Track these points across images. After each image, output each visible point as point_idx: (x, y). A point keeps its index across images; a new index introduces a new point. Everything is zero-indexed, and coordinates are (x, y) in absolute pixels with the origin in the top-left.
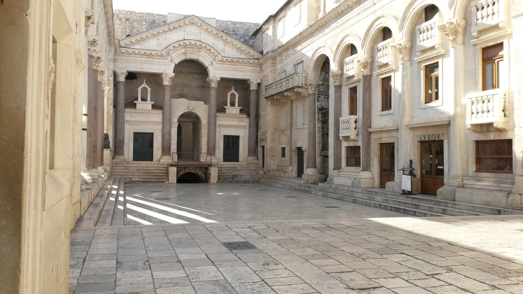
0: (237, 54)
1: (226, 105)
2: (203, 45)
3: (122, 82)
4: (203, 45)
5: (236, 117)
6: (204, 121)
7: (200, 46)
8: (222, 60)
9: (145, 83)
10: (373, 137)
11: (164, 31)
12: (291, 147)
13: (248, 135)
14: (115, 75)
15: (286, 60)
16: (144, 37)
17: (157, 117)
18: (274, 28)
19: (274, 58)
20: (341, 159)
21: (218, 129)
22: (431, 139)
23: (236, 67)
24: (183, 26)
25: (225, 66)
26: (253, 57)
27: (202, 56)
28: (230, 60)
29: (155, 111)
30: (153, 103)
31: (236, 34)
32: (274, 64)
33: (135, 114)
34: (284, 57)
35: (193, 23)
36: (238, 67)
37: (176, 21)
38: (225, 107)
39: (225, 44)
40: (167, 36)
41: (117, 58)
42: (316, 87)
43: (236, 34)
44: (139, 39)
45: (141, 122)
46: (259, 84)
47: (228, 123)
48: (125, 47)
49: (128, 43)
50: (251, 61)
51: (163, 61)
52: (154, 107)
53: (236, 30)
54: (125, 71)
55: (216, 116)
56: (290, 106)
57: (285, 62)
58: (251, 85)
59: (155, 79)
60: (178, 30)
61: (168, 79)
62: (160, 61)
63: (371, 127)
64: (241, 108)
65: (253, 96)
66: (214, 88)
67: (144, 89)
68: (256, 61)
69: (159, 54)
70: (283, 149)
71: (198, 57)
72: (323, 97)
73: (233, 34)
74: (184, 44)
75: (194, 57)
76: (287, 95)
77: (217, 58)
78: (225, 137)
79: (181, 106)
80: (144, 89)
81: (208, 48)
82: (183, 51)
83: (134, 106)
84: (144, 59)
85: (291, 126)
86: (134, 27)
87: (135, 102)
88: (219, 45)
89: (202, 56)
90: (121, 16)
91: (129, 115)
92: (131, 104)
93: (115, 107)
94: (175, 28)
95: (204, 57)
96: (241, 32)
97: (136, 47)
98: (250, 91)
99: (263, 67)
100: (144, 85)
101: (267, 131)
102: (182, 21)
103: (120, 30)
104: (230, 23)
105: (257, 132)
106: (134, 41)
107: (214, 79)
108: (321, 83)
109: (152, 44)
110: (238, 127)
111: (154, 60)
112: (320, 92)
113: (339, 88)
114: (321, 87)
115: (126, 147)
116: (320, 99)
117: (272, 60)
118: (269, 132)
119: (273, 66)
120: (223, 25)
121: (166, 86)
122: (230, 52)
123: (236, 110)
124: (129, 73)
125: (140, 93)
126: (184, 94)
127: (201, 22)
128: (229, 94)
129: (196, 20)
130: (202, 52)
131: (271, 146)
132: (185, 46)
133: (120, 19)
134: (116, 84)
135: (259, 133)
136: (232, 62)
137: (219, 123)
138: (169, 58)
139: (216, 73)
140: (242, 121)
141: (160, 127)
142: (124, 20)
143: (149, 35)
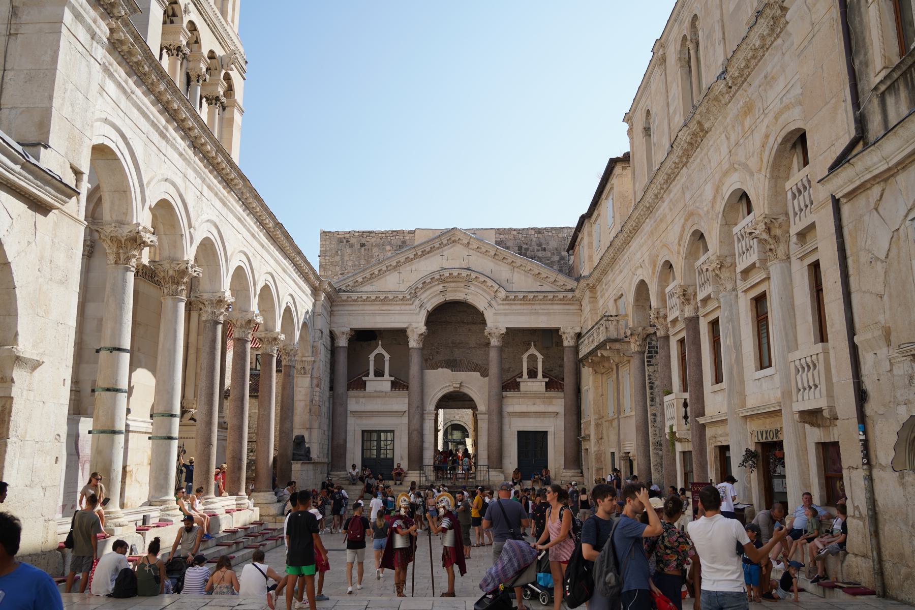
1: (521, 377)
3: (344, 347)
4: (473, 275)
5: (539, 398)
6: (482, 407)
7: (468, 276)
9: (380, 346)
10: (709, 432)
11: (408, 260)
12: (620, 451)
14: (332, 336)
15: (607, 290)
16: (376, 273)
17: (400, 403)
18: (590, 235)
19: (593, 289)
20: (676, 478)
21: (506, 420)
22: (770, 440)
23: (534, 307)
24: (438, 248)
25: (514, 307)
26: (565, 288)
30: (393, 379)
31: (544, 250)
32: (594, 299)
36: (537, 307)
37: (425, 243)
38: (518, 380)
40: (414, 267)
41: (335, 309)
42: (644, 339)
43: (544, 250)
45: (373, 413)
46: (579, 336)
48: (348, 291)
49: (351, 284)
50: (561, 296)
51: (407, 307)
52: (395, 385)
53: (543, 241)
55: (501, 399)
56: (615, 376)
58: (564, 337)
59: (396, 337)
61: (416, 337)
62: (403, 307)
63: (703, 414)
64: (547, 380)
67: (379, 358)
68: (570, 295)
70: (613, 453)
73: (538, 250)
74: (443, 278)
75: (459, 296)
76: (602, 355)
77: (499, 294)
78: (520, 434)
80: (379, 358)
81: (482, 278)
82: (440, 287)
83: (363, 386)
85: (619, 412)
86: (372, 256)
87: (364, 379)
88: (503, 272)
90: (353, 241)
91: (355, 403)
92: (356, 383)
93: (331, 389)
94: (424, 253)
96: (553, 244)
97: (365, 289)
98: (563, 348)
100: (380, 350)
103: (350, 263)
104: (533, 232)
105: (579, 424)
106: (360, 280)
107: (496, 331)
109: (392, 282)
110: (543, 414)
111: (393, 308)
112: (653, 347)
113: (667, 338)
116: (653, 361)
119: (593, 302)
120: (520, 236)
122: (522, 281)
125: (372, 363)
126: (455, 360)
128: (525, 357)
130: (473, 288)
131: (595, 449)
132: (442, 280)
133: (352, 246)
134: (333, 350)
136: (527, 299)
138: (417, 302)
139: (498, 320)
141: (405, 420)
142: (357, 246)
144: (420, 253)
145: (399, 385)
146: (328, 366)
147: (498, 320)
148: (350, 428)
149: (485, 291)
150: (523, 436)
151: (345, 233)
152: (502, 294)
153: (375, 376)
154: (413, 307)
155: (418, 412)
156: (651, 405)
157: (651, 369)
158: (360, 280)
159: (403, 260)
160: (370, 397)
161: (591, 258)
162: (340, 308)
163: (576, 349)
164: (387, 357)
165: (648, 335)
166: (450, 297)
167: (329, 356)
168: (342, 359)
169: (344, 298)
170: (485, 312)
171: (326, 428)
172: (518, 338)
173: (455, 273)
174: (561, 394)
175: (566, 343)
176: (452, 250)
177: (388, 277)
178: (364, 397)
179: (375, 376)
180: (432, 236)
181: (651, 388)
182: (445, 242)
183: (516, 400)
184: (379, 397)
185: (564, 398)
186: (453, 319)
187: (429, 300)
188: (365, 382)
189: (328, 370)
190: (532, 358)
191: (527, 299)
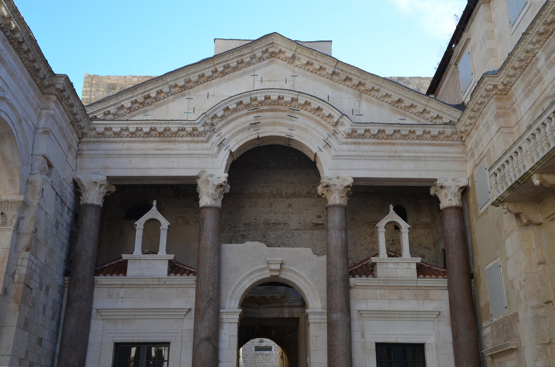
0: (396, 118)
1: (377, 255)
3: (92, 205)
4: (302, 101)
5: (408, 288)
6: (316, 303)
7: (293, 105)
8: (352, 134)
9: (154, 208)
13: (449, 337)
16: (153, 95)
17: (183, 295)
18: (489, 20)
19: (505, 92)
21: (356, 325)
23: (393, 148)
24: (249, 64)
25: (365, 147)
27: (301, 128)
29: (178, 279)
30: (171, 257)
33: (122, 292)
34: (541, 63)
36: (399, 148)
38: (374, 260)
39: (360, 96)
40: (211, 91)
41: (84, 147)
44: (140, 98)
45: (136, 313)
46: (465, 191)
47: (384, 306)
49: (113, 110)
51: (199, 145)
52: (174, 268)
54: (102, 178)
55: (347, 288)
57: (548, 77)
59: (179, 193)
61: (211, 190)
62: (192, 145)
64: (419, 260)
65: (451, 223)
66: (339, 206)
68: (449, 131)
69: (189, 129)
71: (289, 132)
77: (341, 129)
79: (246, 264)
81: (315, 104)
82: (251, 118)
83: (121, 268)
84: (149, 146)
87: (125, 256)
89: (301, 128)
93: (67, 273)
95: (305, 130)
99: (470, 143)
100: (153, 213)
101: (516, 315)
102: (246, 51)
106: (127, 104)
107: (336, 182)
110: (417, 316)
111: (177, 146)
117: (498, 99)
118: (526, 316)
121: (204, 207)
122: (373, 112)
123: (404, 268)
124: (117, 186)
125: (139, 233)
128: (381, 225)
134: (78, 210)
135: (487, 331)
136: (380, 135)
137: (357, 306)
138: (215, 139)
140: (427, 298)
141: (189, 324)
143: (166, 89)
144: (220, 69)
146: (64, 234)
147: (340, 167)
148: (93, 338)
149: (319, 123)
150: (384, 350)
151: (120, 78)
152: (346, 127)
153: (144, 253)
154: (208, 145)
155: (208, 308)
158: (127, 104)
159: (194, 78)
160: (130, 286)
161: (492, 52)
162: (92, 146)
163: (461, 211)
164: (165, 223)
166: (266, 131)
167: (67, 218)
168: (90, 222)
169: (100, 129)
170: (319, 154)
171: (46, 335)
173: (274, 97)
174: (443, 282)
175: (444, 203)
176: (269, 68)
177: (170, 105)
178: (122, 286)
179: (144, 253)
180: (238, 44)
182: (259, 54)
183: (370, 292)
185: (450, 288)
186: (269, 166)
187: (233, 136)
188: (126, 262)
189: (66, 242)
191: (380, 135)
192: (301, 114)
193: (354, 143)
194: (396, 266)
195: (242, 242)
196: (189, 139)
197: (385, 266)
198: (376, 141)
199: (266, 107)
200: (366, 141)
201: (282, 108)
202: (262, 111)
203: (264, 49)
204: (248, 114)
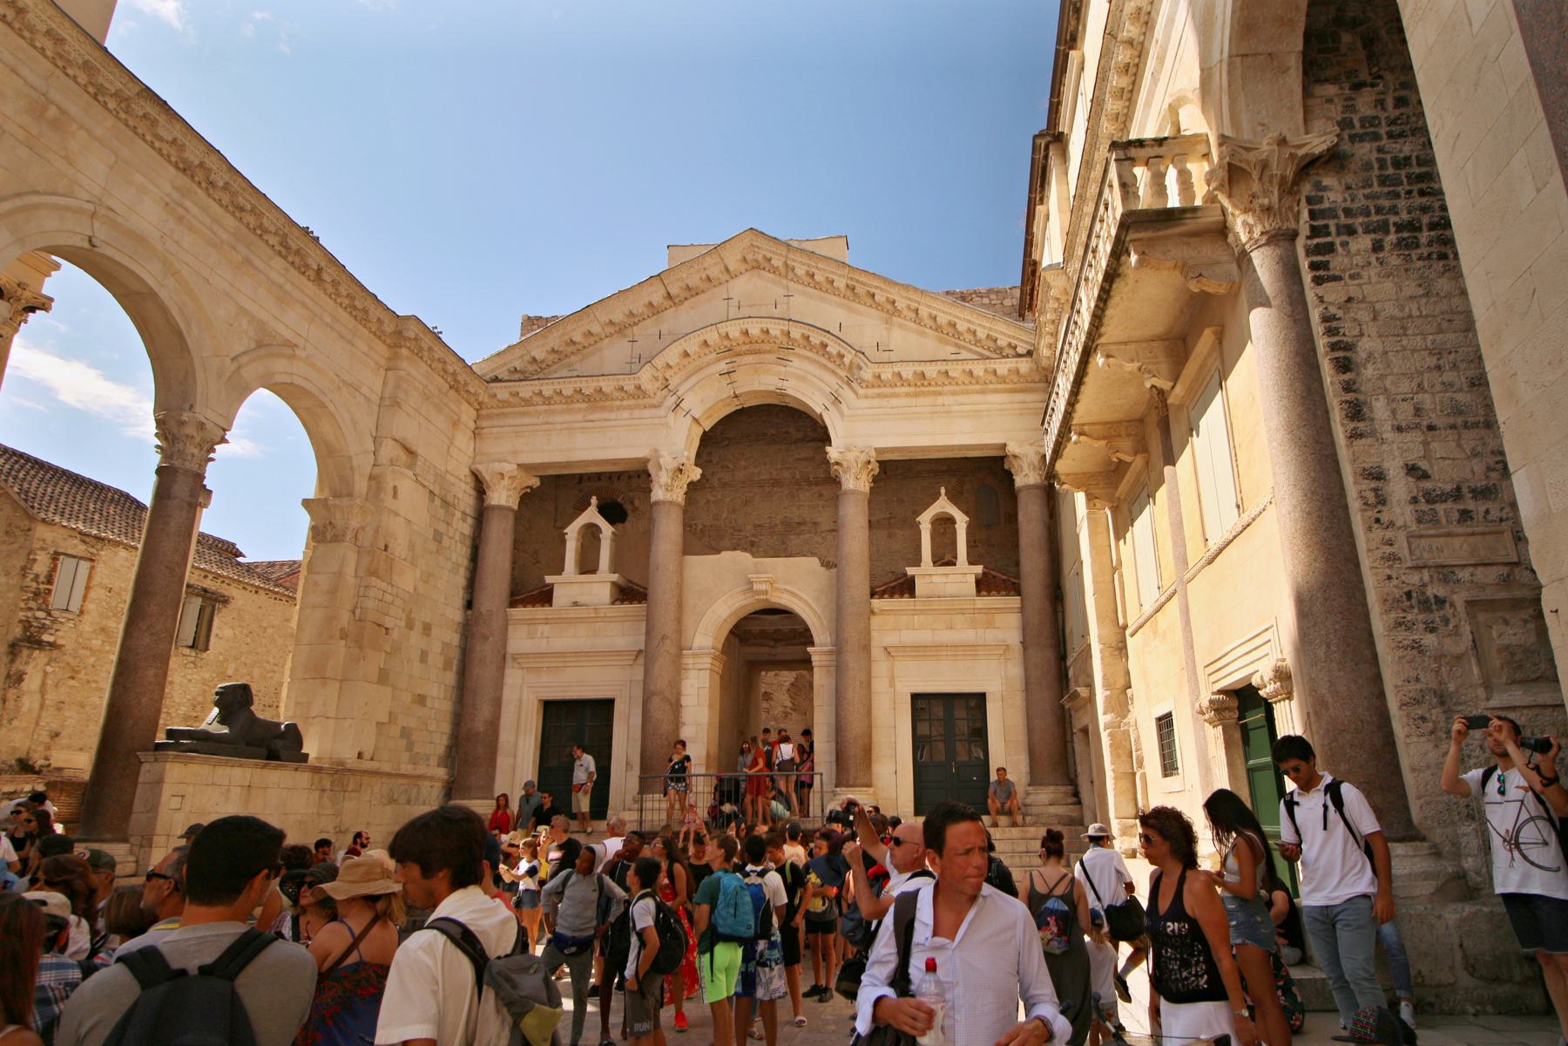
2: (796, 333)
5: (962, 612)
25: (895, 402)
28: (908, 371)
30: (615, 577)
33: (546, 628)
35: (757, 267)
51: (647, 413)
60: (702, 297)
62: (637, 413)
64: (979, 569)
67: (591, 531)
71: (780, 384)
72: (1363, 242)
80: (591, 531)
81: (816, 338)
83: (545, 597)
87: (549, 579)
95: (803, 379)
100: (591, 515)
107: (851, 456)
108: (1318, 142)
111: (613, 416)
112: (1331, 213)
114: (1327, 181)
115: (502, 762)
116: (1337, 262)
127: (784, 251)
128: (925, 520)
129: (766, 249)
130: (796, 362)
145: (629, 593)
148: (509, 695)
156: (1354, 435)
157: (1334, 293)
164: (607, 529)
165: (1309, 166)
172: (903, 477)
174: (1014, 601)
178: (547, 621)
181: (1344, 366)
184: (581, 620)
190: (944, 524)
192: (798, 355)
193: (878, 396)
194: (944, 579)
195: (718, 552)
196: (632, 402)
197: (927, 579)
198: (912, 389)
199: (744, 348)
200: (897, 390)
201: (766, 347)
202: (739, 355)
203: (739, 257)
204: (719, 360)
